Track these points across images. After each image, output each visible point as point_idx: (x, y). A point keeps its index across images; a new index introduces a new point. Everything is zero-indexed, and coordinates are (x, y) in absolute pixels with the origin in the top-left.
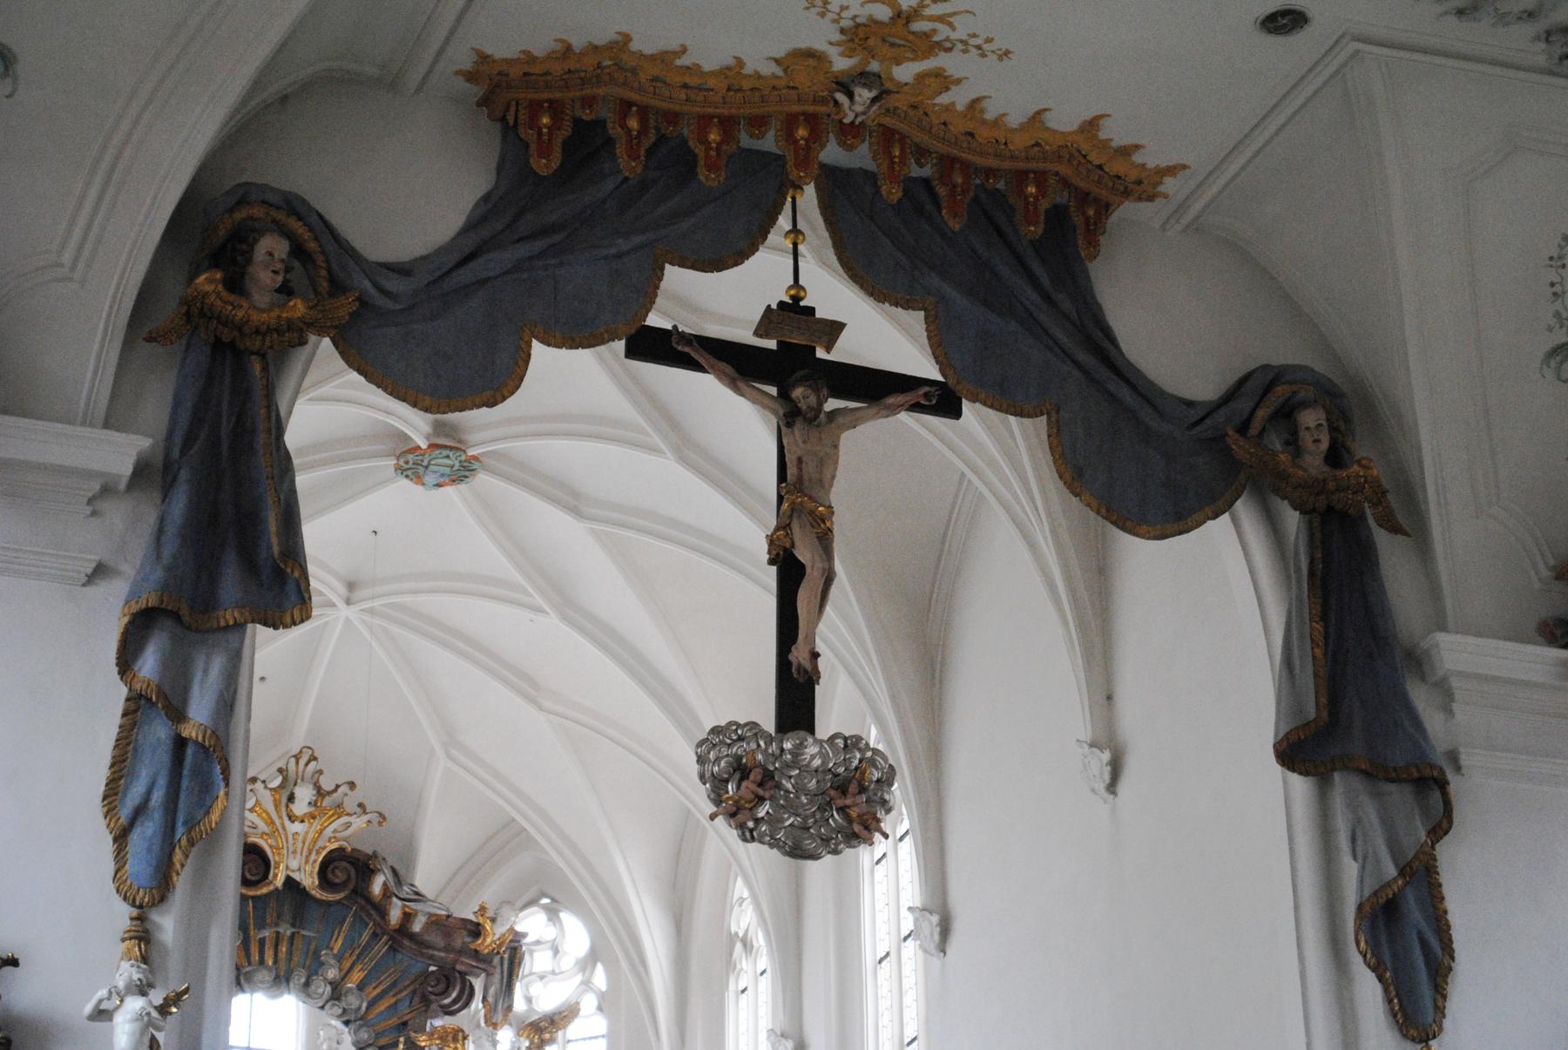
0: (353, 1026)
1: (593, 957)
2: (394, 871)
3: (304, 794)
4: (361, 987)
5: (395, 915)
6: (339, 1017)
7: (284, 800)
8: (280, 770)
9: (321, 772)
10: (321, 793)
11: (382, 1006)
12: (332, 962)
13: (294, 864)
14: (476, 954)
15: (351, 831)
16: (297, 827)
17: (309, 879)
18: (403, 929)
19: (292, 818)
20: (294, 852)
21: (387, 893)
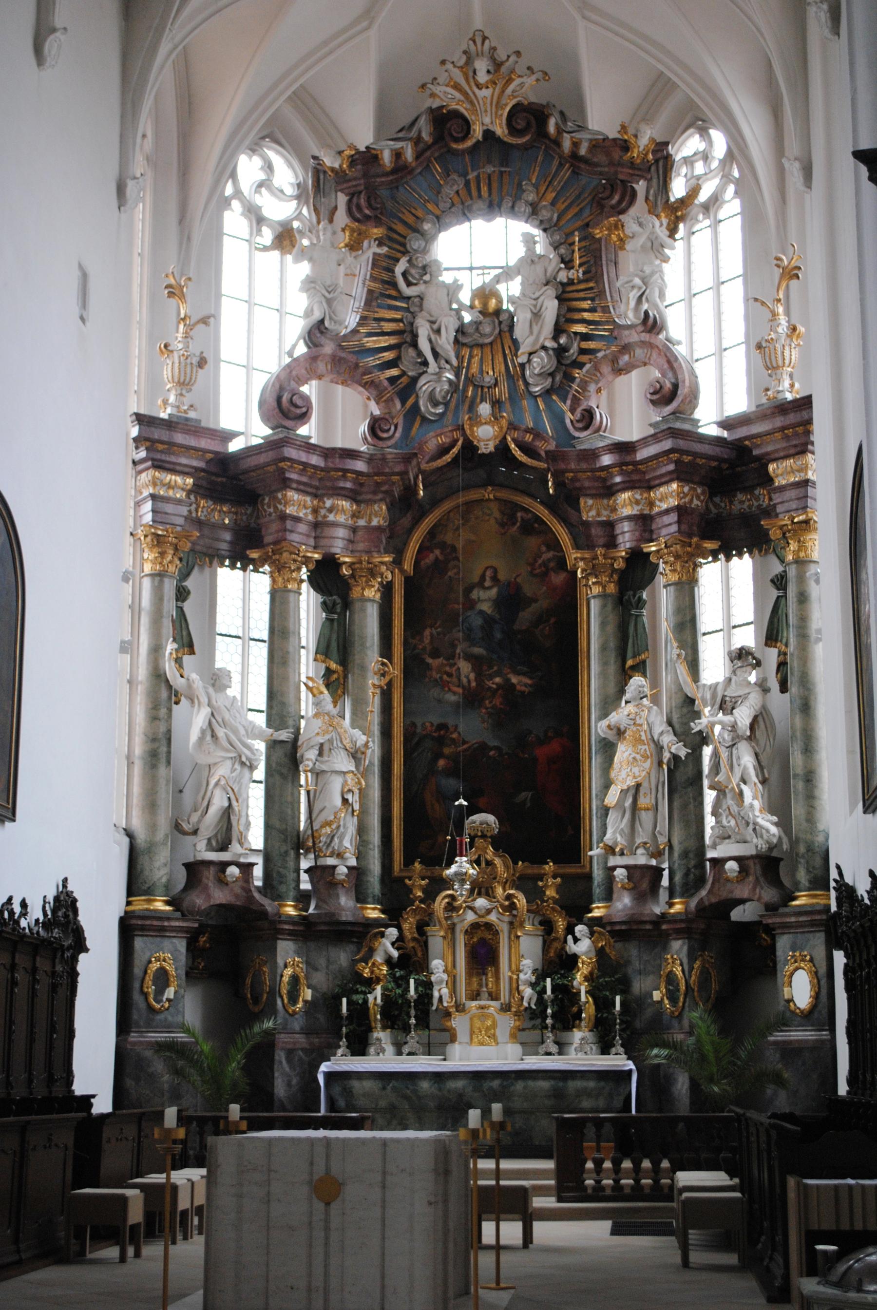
0: (549, 232)
2: (562, 113)
3: (482, 66)
4: (553, 204)
5: (567, 144)
6: (538, 227)
7: (471, 74)
8: (465, 52)
9: (494, 49)
10: (498, 65)
11: (569, 215)
12: (530, 188)
13: (487, 120)
14: (632, 164)
15: (526, 89)
16: (485, 93)
17: (500, 130)
18: (574, 155)
19: (479, 86)
20: (486, 111)
21: (560, 131)
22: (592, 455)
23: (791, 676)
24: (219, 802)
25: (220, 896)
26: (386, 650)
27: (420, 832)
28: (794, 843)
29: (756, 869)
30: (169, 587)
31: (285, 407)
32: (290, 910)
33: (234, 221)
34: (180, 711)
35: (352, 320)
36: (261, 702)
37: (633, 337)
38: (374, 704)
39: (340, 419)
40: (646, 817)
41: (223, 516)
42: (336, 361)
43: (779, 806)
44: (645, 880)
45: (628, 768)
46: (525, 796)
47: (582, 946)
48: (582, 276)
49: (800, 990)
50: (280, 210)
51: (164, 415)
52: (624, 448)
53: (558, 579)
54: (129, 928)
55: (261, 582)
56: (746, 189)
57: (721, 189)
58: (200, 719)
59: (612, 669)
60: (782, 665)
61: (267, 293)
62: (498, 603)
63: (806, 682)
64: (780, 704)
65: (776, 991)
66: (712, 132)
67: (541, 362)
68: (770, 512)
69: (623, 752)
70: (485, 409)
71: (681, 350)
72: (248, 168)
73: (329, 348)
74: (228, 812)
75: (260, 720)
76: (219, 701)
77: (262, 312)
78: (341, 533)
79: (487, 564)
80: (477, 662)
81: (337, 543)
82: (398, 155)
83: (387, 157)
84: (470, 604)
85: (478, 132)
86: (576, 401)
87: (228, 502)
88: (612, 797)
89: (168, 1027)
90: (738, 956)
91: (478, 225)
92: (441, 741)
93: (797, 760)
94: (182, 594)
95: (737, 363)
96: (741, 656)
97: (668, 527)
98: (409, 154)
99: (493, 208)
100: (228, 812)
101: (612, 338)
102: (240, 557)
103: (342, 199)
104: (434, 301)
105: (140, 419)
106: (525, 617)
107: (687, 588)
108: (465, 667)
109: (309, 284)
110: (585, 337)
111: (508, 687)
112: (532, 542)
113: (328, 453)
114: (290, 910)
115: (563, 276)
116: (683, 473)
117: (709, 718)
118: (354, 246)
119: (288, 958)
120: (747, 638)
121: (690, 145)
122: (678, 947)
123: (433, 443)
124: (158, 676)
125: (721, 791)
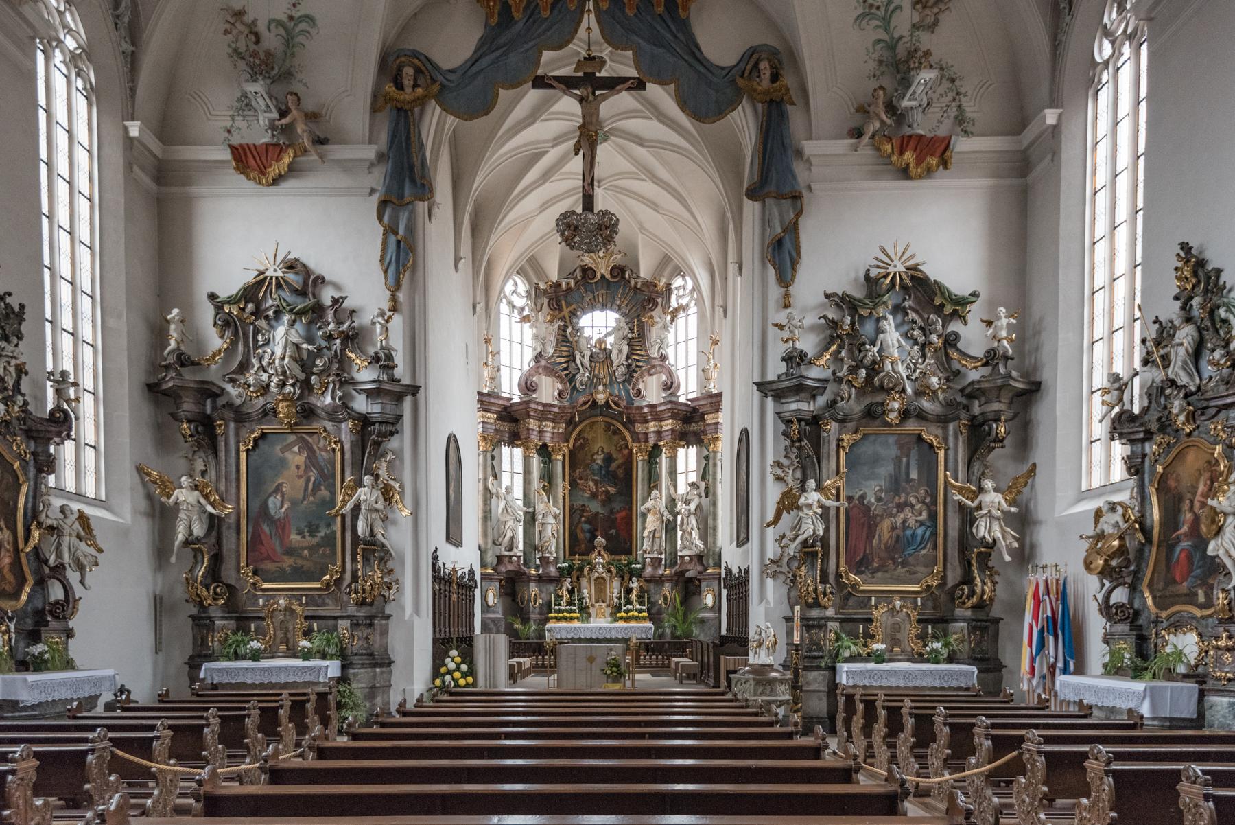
1: (693, 290)
5: (633, 283)
15: (617, 259)
17: (608, 276)
22: (640, 408)
23: (709, 492)
24: (509, 534)
25: (510, 567)
26: (564, 480)
27: (578, 544)
28: (709, 551)
29: (695, 559)
30: (489, 456)
31: (528, 387)
32: (533, 572)
33: (504, 308)
34: (494, 500)
35: (551, 352)
36: (521, 497)
37: (657, 363)
38: (561, 500)
39: (548, 391)
40: (658, 541)
41: (506, 427)
42: (546, 368)
43: (704, 537)
44: (656, 562)
45: (652, 523)
46: (613, 531)
47: (635, 585)
48: (637, 337)
49: (709, 600)
50: (520, 302)
51: (485, 391)
52: (652, 406)
53: (626, 452)
54: (485, 577)
55: (518, 452)
56: (700, 302)
57: (690, 302)
58: (502, 505)
59: (646, 487)
60: (706, 488)
61: (516, 337)
62: (604, 460)
63: (715, 494)
64: (705, 501)
65: (701, 600)
66: (688, 278)
67: (622, 370)
68: (704, 432)
69: (650, 518)
70: (601, 388)
71: (673, 368)
72: (509, 287)
73: (543, 363)
74: (512, 538)
75: (520, 503)
76: (509, 498)
77: (518, 345)
78: (548, 435)
79: (600, 445)
80: (596, 482)
81: (547, 439)
82: (568, 284)
83: (564, 285)
84: (593, 461)
85: (599, 276)
86: (634, 386)
87: (509, 422)
88: (645, 534)
89: (494, 612)
90: (689, 588)
91: (597, 314)
92: (583, 511)
93: (710, 522)
94: (493, 458)
95: (693, 372)
96: (693, 484)
97: (667, 437)
98: (572, 284)
99: (604, 307)
100: (512, 538)
101: (648, 362)
102: (511, 443)
103: (546, 301)
104: (583, 343)
105: (479, 393)
106: (613, 466)
107: (673, 459)
108: (591, 484)
109: (535, 337)
110: (638, 361)
111: (607, 492)
112: (616, 437)
113: (545, 405)
114: (533, 572)
115: (630, 336)
116: (673, 417)
117: (680, 506)
118: (551, 321)
119: (533, 588)
120: (693, 477)
121: (677, 282)
122: (668, 585)
123: (581, 400)
124: (486, 489)
125: (684, 532)
